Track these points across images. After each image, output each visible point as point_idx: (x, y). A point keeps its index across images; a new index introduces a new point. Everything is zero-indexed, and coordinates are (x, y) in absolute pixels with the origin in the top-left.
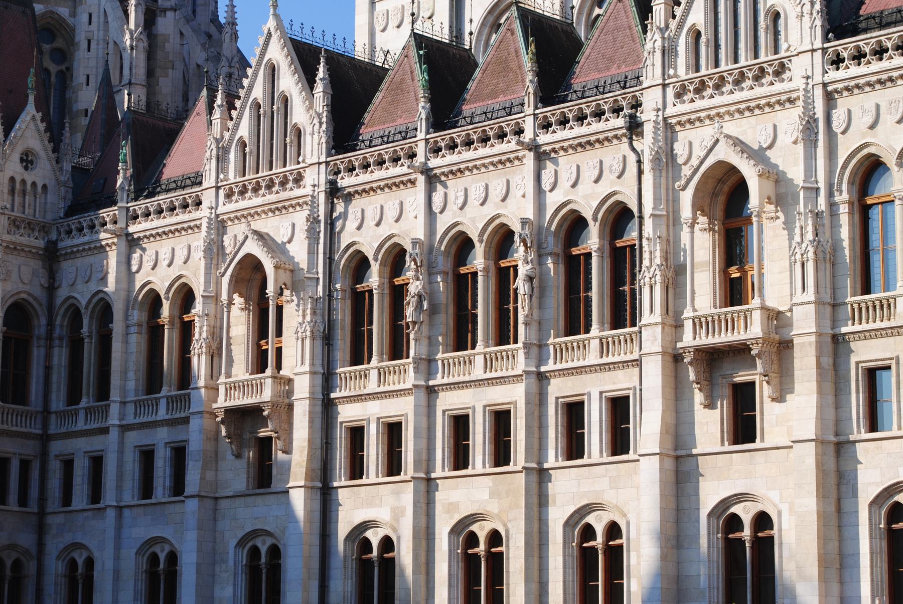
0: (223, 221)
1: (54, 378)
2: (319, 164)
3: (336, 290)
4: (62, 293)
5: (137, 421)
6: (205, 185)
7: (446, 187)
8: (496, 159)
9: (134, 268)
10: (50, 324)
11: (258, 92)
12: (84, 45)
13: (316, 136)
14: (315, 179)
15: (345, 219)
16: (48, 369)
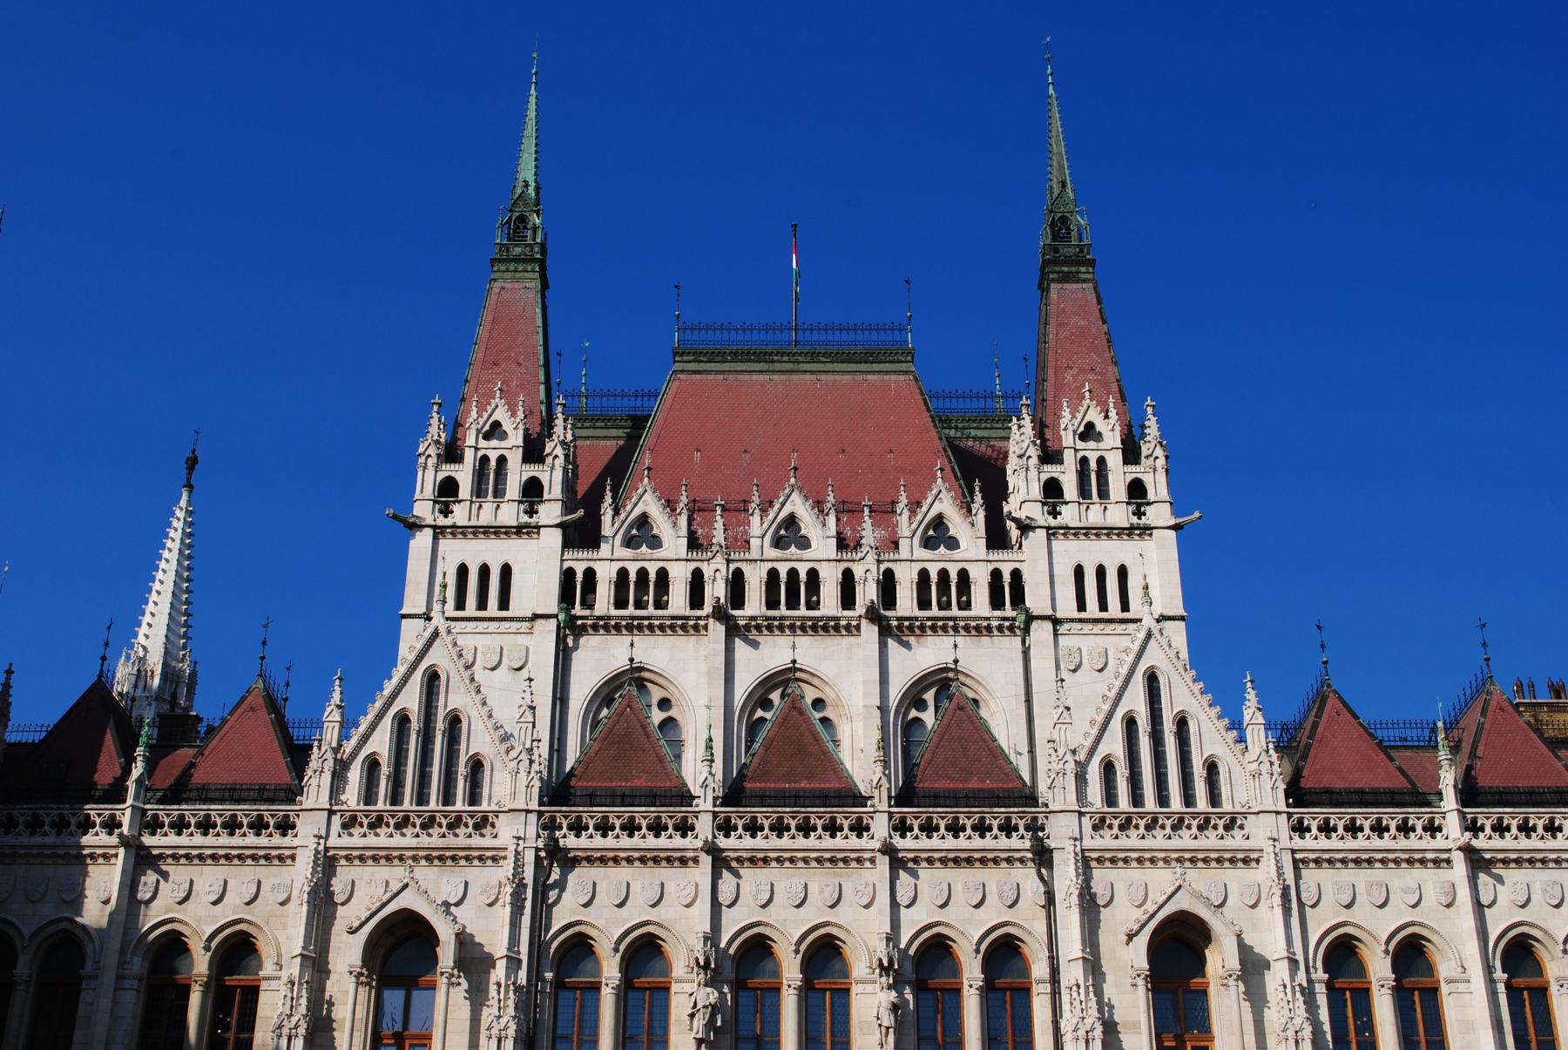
0: (335, 858)
2: (528, 811)
3: (544, 980)
7: (738, 876)
8: (827, 855)
9: (144, 894)
13: (523, 775)
15: (563, 889)
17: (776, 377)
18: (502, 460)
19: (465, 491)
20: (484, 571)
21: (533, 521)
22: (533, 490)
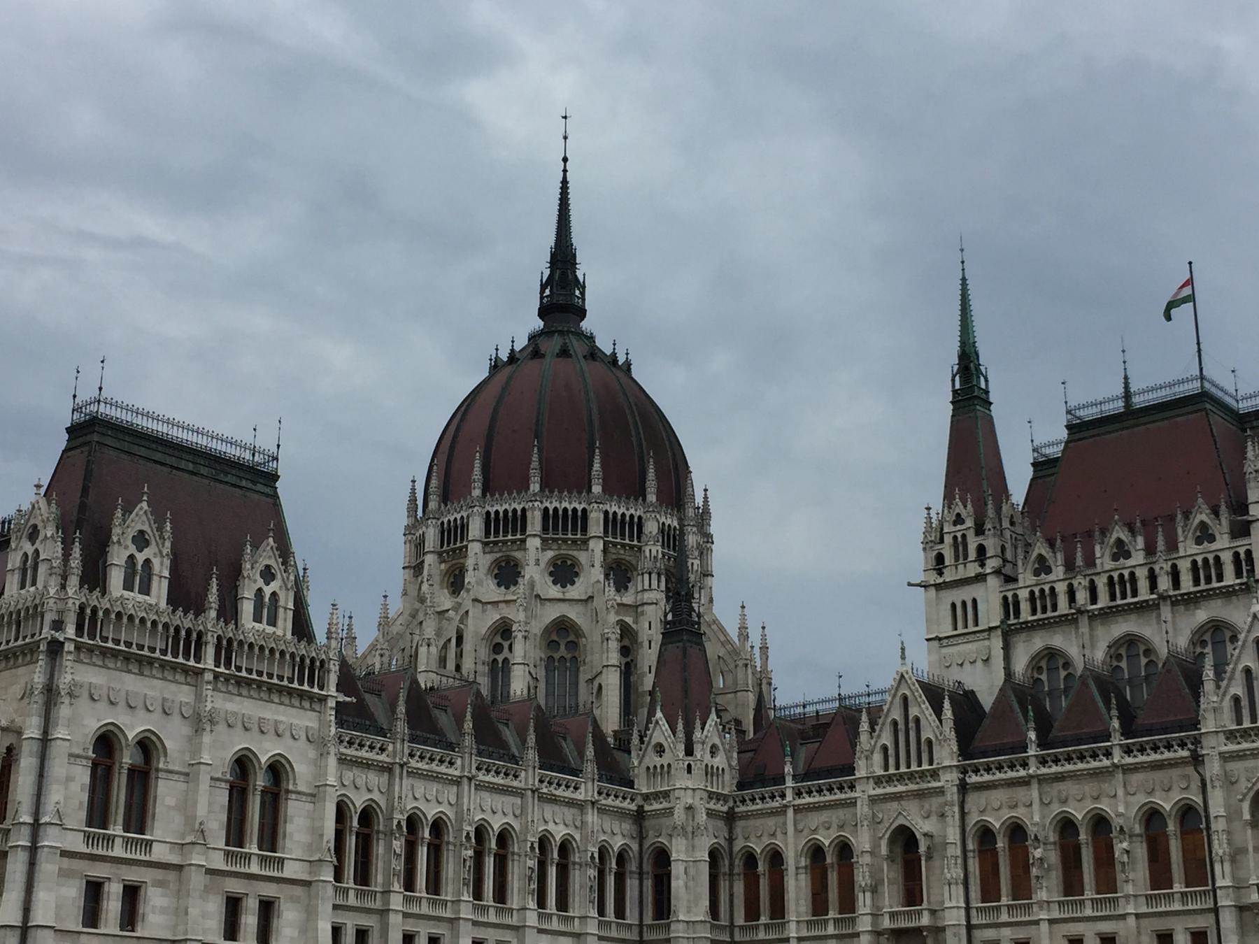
1: (736, 901)
4: (739, 844)
5: (809, 934)
6: (858, 775)
10: (731, 865)
11: (897, 715)
12: (646, 644)
14: (949, 779)
16: (731, 895)
18: (964, 536)
20: (964, 604)
22: (981, 550)
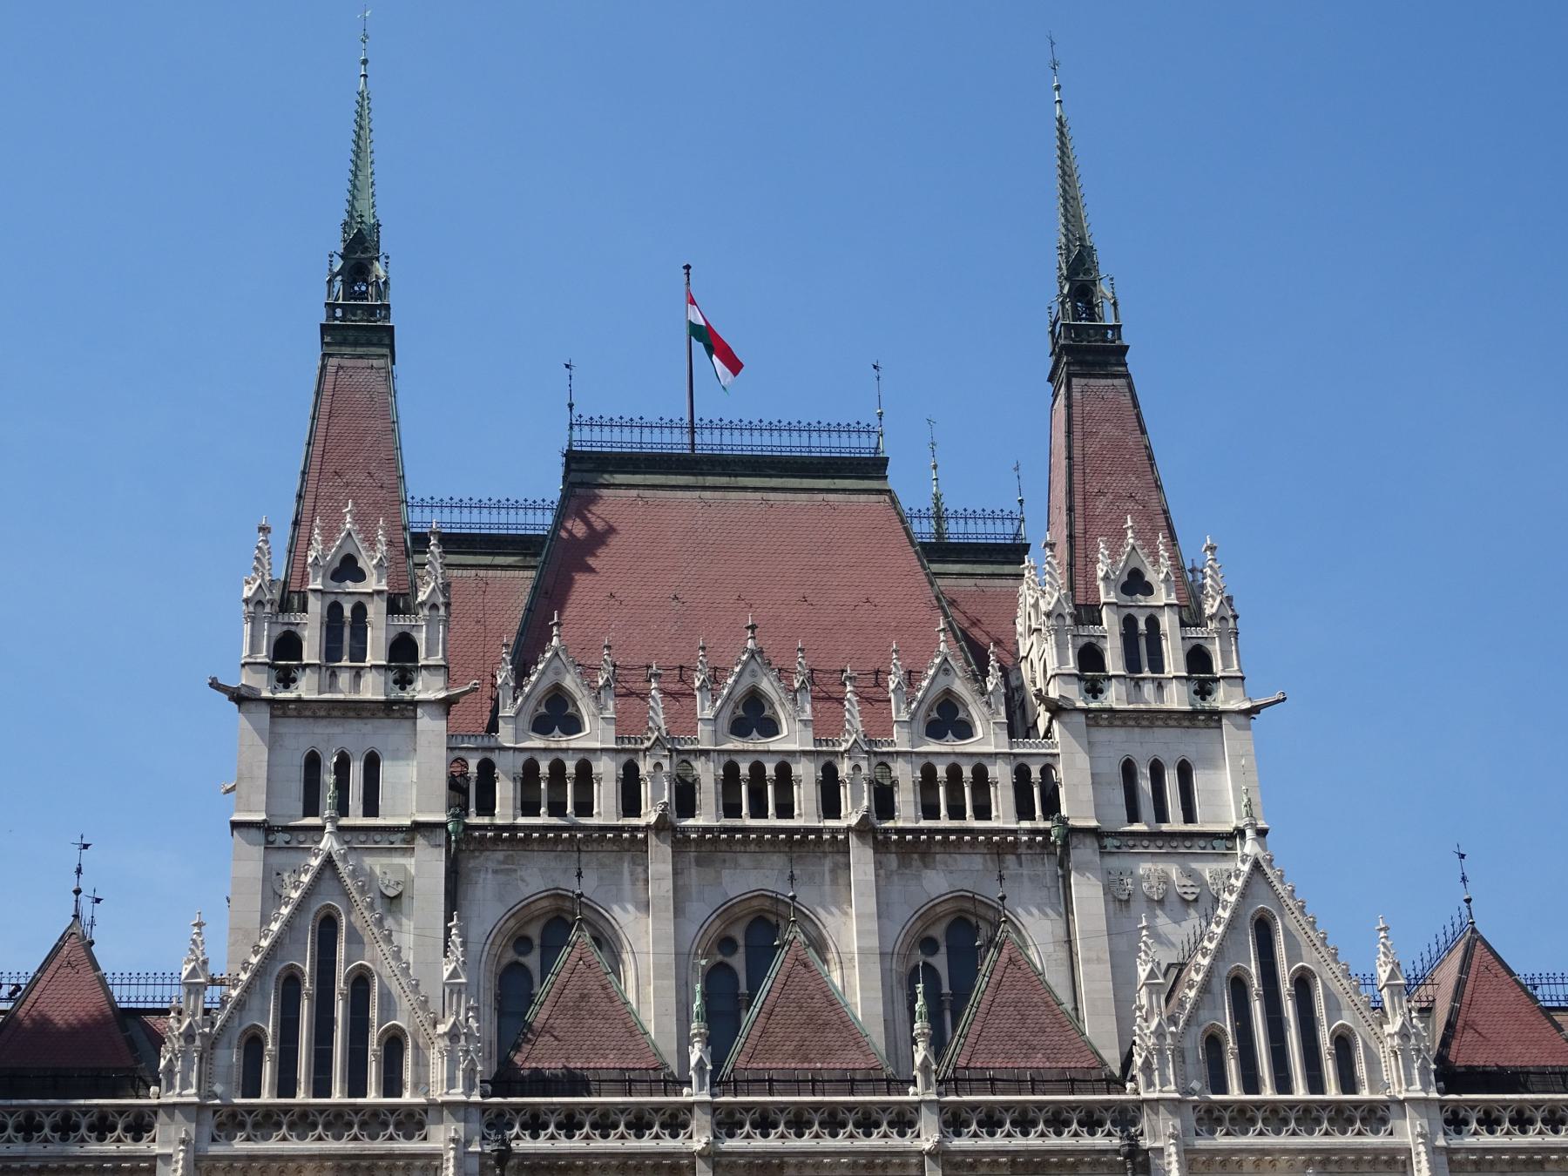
17: (707, 494)
19: (311, 651)
21: (406, 695)
